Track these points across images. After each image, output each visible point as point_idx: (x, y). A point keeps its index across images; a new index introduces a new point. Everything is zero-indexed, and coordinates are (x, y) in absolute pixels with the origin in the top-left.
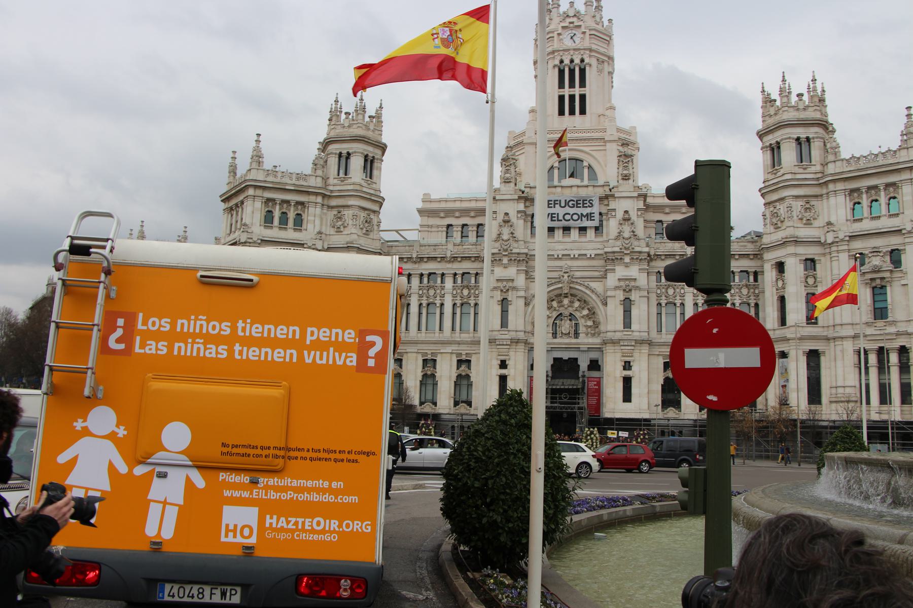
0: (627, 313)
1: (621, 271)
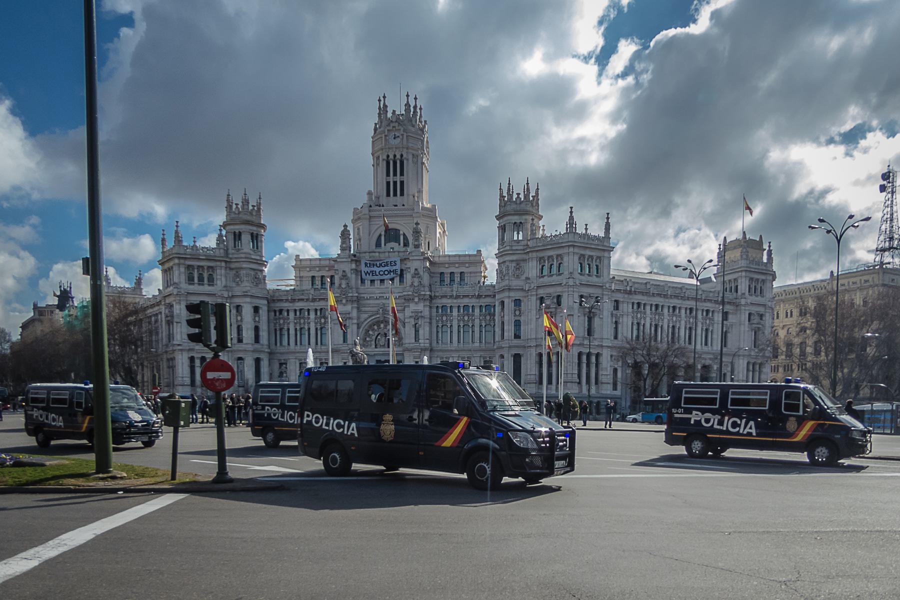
0: (417, 331)
1: (413, 307)
